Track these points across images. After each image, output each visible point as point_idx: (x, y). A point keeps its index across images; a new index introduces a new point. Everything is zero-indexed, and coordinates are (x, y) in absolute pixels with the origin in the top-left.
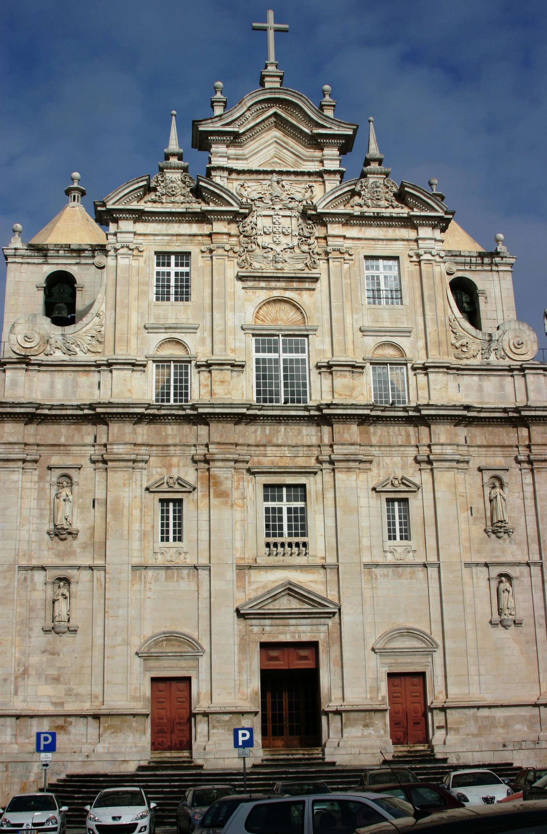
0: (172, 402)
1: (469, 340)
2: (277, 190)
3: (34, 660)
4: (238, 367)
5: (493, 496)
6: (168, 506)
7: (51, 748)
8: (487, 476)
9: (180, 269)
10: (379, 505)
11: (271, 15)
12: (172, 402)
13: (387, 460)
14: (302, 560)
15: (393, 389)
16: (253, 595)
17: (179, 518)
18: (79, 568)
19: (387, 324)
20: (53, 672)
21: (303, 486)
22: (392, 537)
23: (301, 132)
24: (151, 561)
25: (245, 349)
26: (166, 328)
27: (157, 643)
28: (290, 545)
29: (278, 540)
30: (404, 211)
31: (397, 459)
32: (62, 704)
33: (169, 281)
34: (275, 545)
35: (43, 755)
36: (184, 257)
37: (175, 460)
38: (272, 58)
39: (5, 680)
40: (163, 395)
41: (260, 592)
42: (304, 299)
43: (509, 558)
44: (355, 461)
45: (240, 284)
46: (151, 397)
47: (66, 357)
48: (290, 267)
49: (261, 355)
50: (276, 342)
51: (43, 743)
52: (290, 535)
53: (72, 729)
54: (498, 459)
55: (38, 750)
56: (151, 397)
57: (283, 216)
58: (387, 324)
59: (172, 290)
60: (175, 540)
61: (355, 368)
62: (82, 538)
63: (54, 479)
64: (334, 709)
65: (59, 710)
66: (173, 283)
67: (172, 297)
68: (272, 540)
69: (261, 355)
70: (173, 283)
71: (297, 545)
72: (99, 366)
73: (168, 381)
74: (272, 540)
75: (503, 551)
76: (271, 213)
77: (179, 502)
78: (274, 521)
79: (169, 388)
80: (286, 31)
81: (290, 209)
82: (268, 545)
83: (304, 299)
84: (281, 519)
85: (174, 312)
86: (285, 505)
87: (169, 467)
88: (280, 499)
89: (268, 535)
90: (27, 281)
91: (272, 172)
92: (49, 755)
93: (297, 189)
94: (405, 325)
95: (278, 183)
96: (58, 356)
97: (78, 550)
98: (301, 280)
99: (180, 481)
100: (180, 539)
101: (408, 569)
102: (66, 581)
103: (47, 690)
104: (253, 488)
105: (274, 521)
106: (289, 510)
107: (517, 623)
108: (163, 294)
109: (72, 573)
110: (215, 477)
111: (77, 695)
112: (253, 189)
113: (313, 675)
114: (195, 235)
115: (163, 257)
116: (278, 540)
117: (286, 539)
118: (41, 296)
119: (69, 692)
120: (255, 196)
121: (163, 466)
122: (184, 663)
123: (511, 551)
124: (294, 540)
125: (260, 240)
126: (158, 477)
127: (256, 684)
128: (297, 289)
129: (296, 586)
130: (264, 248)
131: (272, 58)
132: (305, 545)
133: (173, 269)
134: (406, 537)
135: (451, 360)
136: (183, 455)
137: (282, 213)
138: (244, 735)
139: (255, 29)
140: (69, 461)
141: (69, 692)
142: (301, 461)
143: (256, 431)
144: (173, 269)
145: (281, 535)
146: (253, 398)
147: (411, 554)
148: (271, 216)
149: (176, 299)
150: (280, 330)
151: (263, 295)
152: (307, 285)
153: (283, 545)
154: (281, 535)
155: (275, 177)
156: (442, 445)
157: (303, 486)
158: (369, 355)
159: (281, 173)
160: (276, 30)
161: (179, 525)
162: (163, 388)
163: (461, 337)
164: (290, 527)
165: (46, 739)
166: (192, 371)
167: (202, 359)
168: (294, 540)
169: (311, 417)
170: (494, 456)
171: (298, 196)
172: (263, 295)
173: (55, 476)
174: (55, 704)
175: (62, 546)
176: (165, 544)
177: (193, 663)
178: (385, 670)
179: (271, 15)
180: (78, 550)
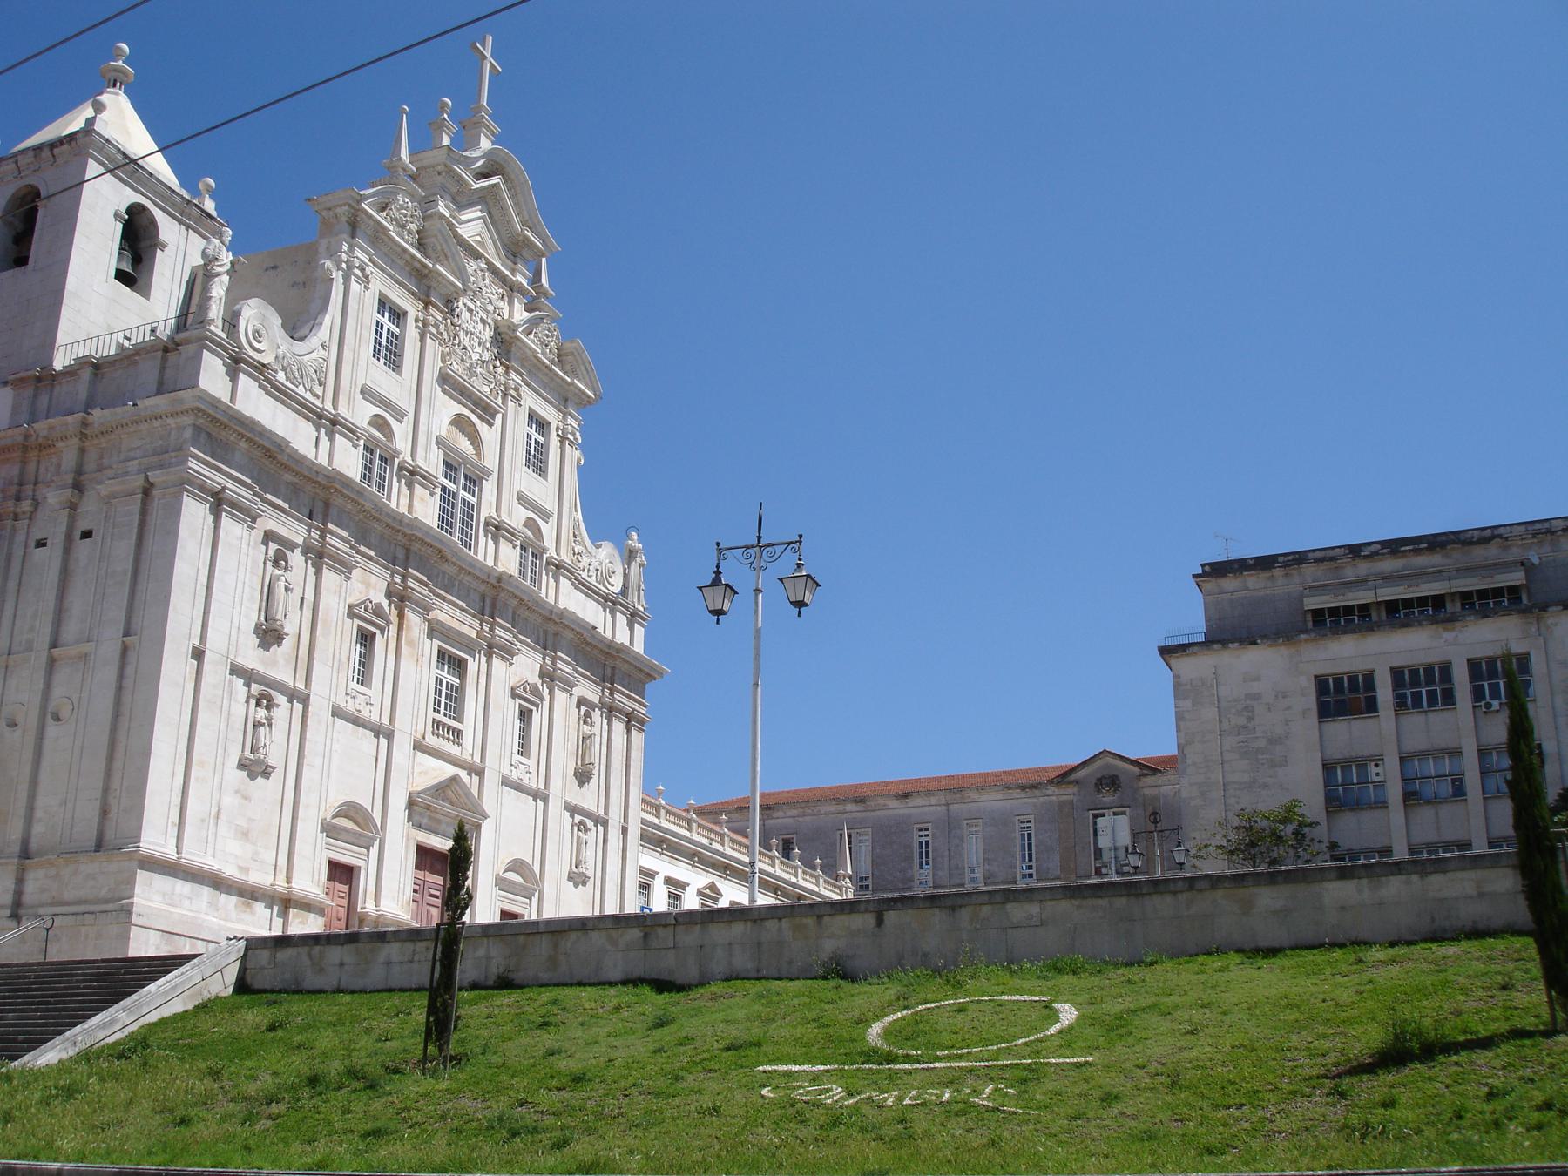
3: (229, 800)
10: (513, 707)
14: (453, 749)
20: (242, 822)
25: (431, 461)
27: (334, 817)
39: (203, 821)
62: (288, 643)
71: (454, 730)
72: (320, 417)
83: (482, 428)
96: (281, 376)
97: (282, 662)
103: (234, 846)
104: (430, 648)
121: (363, 583)
125: (462, 334)
132: (460, 733)
134: (521, 753)
172: (456, 408)
173: (273, 547)
174: (240, 868)
180: (282, 662)
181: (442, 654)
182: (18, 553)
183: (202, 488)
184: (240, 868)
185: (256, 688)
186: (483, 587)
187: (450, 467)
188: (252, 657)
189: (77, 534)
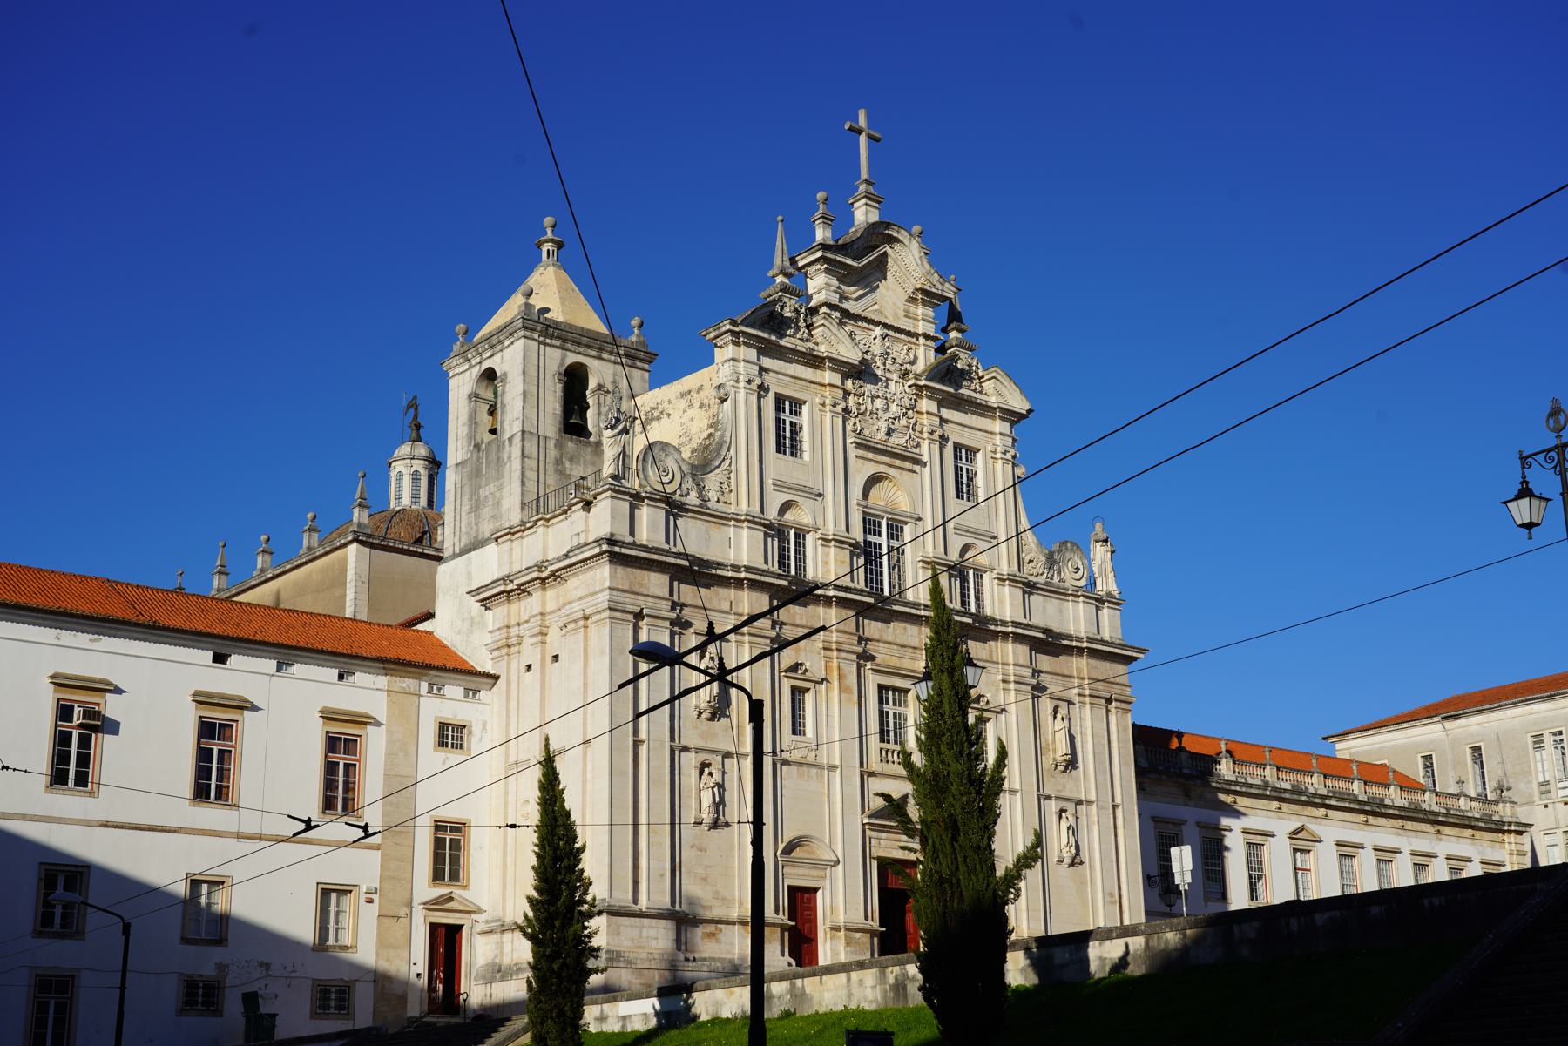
38: (864, 175)
53: (721, 936)
74: (885, 745)
91: (877, 323)
122: (814, 872)
131: (864, 175)
142: (907, 664)
151: (872, 469)
152: (907, 465)
159: (886, 326)
182: (514, 678)
189: (549, 659)
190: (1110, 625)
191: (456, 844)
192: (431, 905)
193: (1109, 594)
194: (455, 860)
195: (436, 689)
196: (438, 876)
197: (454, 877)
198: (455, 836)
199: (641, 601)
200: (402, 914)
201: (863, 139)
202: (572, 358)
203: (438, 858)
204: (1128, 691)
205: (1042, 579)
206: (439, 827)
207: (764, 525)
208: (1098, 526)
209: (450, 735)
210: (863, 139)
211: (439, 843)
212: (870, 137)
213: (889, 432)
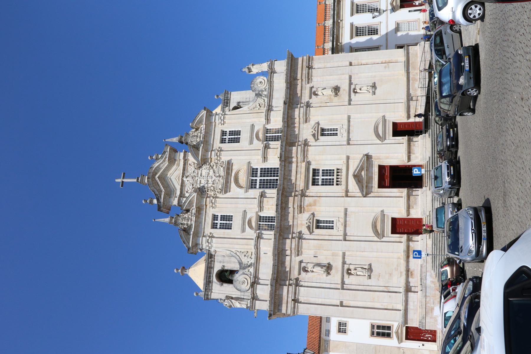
0: (275, 223)
1: (257, 102)
2: (189, 179)
4: (262, 195)
5: (322, 94)
6: (318, 226)
7: (420, 252)
8: (313, 96)
9: (219, 219)
11: (117, 180)
12: (275, 223)
13: (304, 135)
15: (275, 133)
16: (358, 191)
17: (324, 222)
18: (344, 263)
19: (249, 135)
21: (314, 170)
22: (336, 134)
23: (166, 167)
24: (342, 233)
25: (256, 193)
26: (244, 225)
28: (338, 175)
29: (335, 181)
30: (203, 127)
31: (304, 132)
32: (401, 272)
33: (223, 224)
34: (337, 181)
35: (423, 256)
36: (215, 217)
37: (299, 222)
39: (390, 297)
40: (271, 228)
41: (357, 187)
42: (235, 169)
43: (347, 88)
44: (304, 148)
45: (228, 195)
46: (272, 233)
47: (253, 267)
48: (222, 173)
49: (258, 186)
50: (252, 180)
51: (417, 256)
52: (333, 175)
54: (306, 93)
55: (420, 258)
56: (272, 233)
57: (201, 175)
58: (249, 134)
59: (228, 222)
60: (333, 223)
61: (266, 147)
63: (305, 273)
64: (407, 158)
65: (404, 273)
66: (225, 222)
67: (231, 222)
68: (335, 183)
69: (258, 186)
70: (225, 222)
71: (338, 172)
73: (266, 225)
74: (335, 183)
75: (344, 90)
76: (199, 180)
77: (318, 221)
78: (327, 182)
79: (268, 225)
80: (124, 173)
81: (198, 174)
82: (337, 184)
84: (326, 179)
85: (236, 223)
86: (320, 178)
87: (302, 225)
88: (318, 179)
89: (333, 185)
90: (219, 291)
91: (182, 180)
92: (423, 253)
93: (191, 169)
94: (249, 128)
95: (187, 177)
96: (252, 270)
98: (228, 169)
99: (309, 219)
100: (333, 221)
101: (351, 128)
102: (349, 269)
104: (313, 190)
105: (327, 182)
106: (323, 176)
107: (374, 86)
108: (229, 227)
109: (346, 267)
110: (307, 206)
111: (397, 266)
112: (188, 188)
113: (392, 167)
114: (206, 212)
115: (214, 226)
116: (335, 181)
117: (335, 177)
118: (225, 285)
119: (396, 269)
120: (191, 187)
123: (344, 87)
124: (335, 174)
126: (306, 229)
127: (395, 191)
128: (232, 171)
129: (354, 172)
130: (213, 184)
132: (338, 169)
133: (219, 222)
135: (264, 110)
136: (297, 219)
137: (199, 175)
138: (416, 171)
139: (122, 186)
140: (297, 267)
141: (396, 269)
143: (289, 188)
144: (219, 222)
145: (333, 179)
146: (275, 191)
147: (344, 126)
148: (200, 181)
149: (232, 221)
150: (248, 178)
151: (233, 185)
153: (337, 178)
154: (333, 179)
155: (185, 179)
156: (299, 113)
157: (314, 170)
158: (261, 142)
159: (183, 177)
160: (123, 178)
161: (327, 222)
162: (269, 227)
163: (256, 105)
164: (330, 176)
165: (416, 254)
166: (262, 214)
167: (257, 209)
168: (335, 174)
169: (285, 166)
170: (305, 93)
171: (193, 169)
172: (233, 185)
173: (303, 274)
174: (401, 276)
175: (333, 272)
176: (335, 227)
177: (386, 216)
178: (391, 137)
179: (117, 180)
181: (314, 184)
183: (294, 307)
184: (401, 276)
185: (346, 276)
186: (287, 164)
187: (252, 185)
188: (336, 277)
190: (281, 66)
191: (379, 327)
192: (400, 341)
193: (269, 66)
194: (384, 327)
195: (328, 332)
196: (389, 335)
197: (389, 328)
198: (375, 327)
199: (290, 300)
200: (402, 351)
201: (125, 180)
202: (214, 279)
203: (383, 335)
204: (305, 58)
205: (266, 99)
206: (372, 334)
207: (258, 239)
208: (244, 70)
209: (342, 328)
210: (125, 180)
211: (378, 334)
212: (123, 178)
213: (220, 176)
